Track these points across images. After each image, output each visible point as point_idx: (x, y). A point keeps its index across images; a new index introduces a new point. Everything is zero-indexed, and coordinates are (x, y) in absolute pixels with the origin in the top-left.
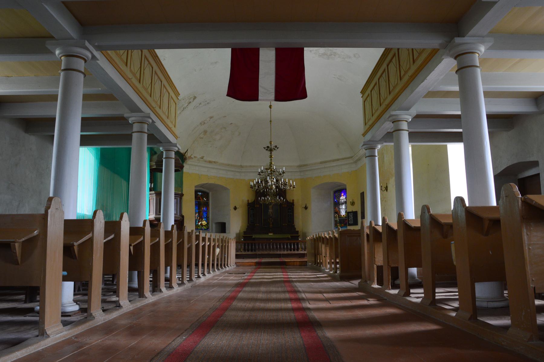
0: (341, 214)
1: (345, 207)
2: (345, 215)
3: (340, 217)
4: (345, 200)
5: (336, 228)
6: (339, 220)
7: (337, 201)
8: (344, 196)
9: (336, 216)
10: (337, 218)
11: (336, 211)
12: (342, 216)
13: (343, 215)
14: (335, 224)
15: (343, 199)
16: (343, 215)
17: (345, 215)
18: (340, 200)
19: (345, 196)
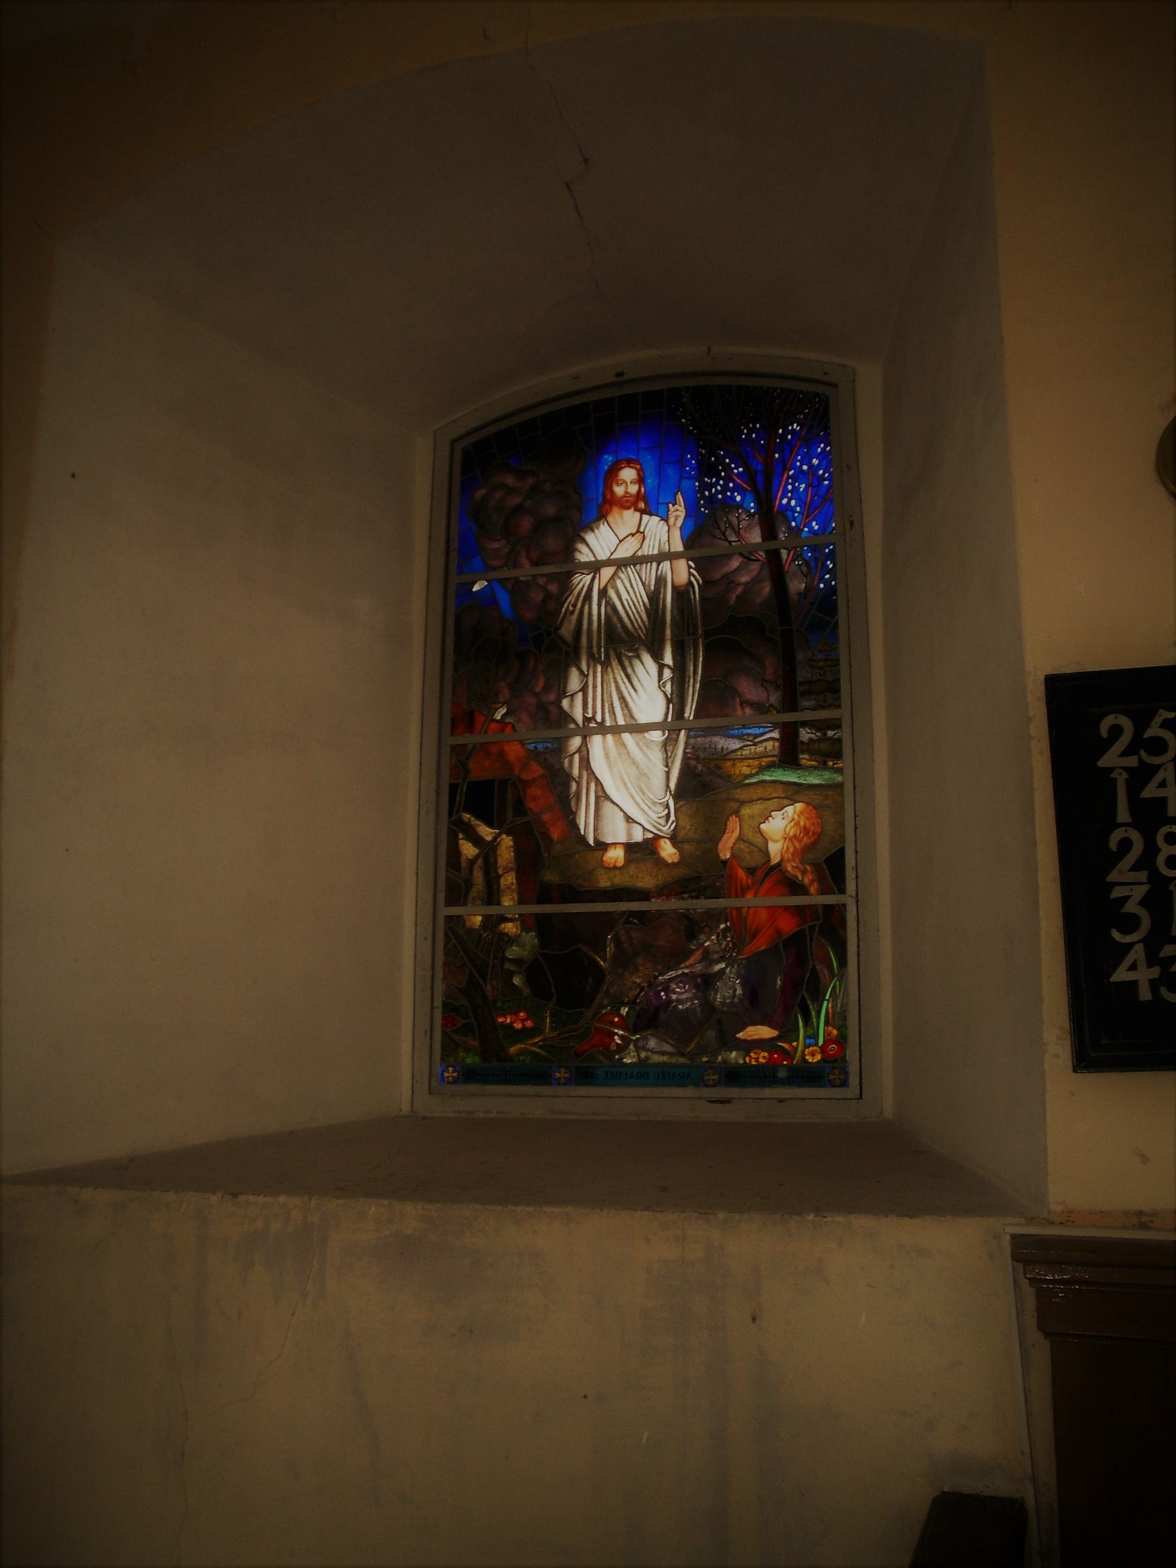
0: (585, 821)
1: (677, 701)
2: (668, 851)
3: (551, 876)
4: (681, 572)
5: (470, 1075)
6: (542, 924)
7: (503, 597)
8: (648, 503)
9: (488, 850)
10: (492, 896)
11: (480, 770)
12: (616, 855)
13: (616, 831)
14: (450, 1010)
15: (635, 561)
16: (616, 831)
17: (668, 851)
18: (582, 581)
19: (678, 512)
